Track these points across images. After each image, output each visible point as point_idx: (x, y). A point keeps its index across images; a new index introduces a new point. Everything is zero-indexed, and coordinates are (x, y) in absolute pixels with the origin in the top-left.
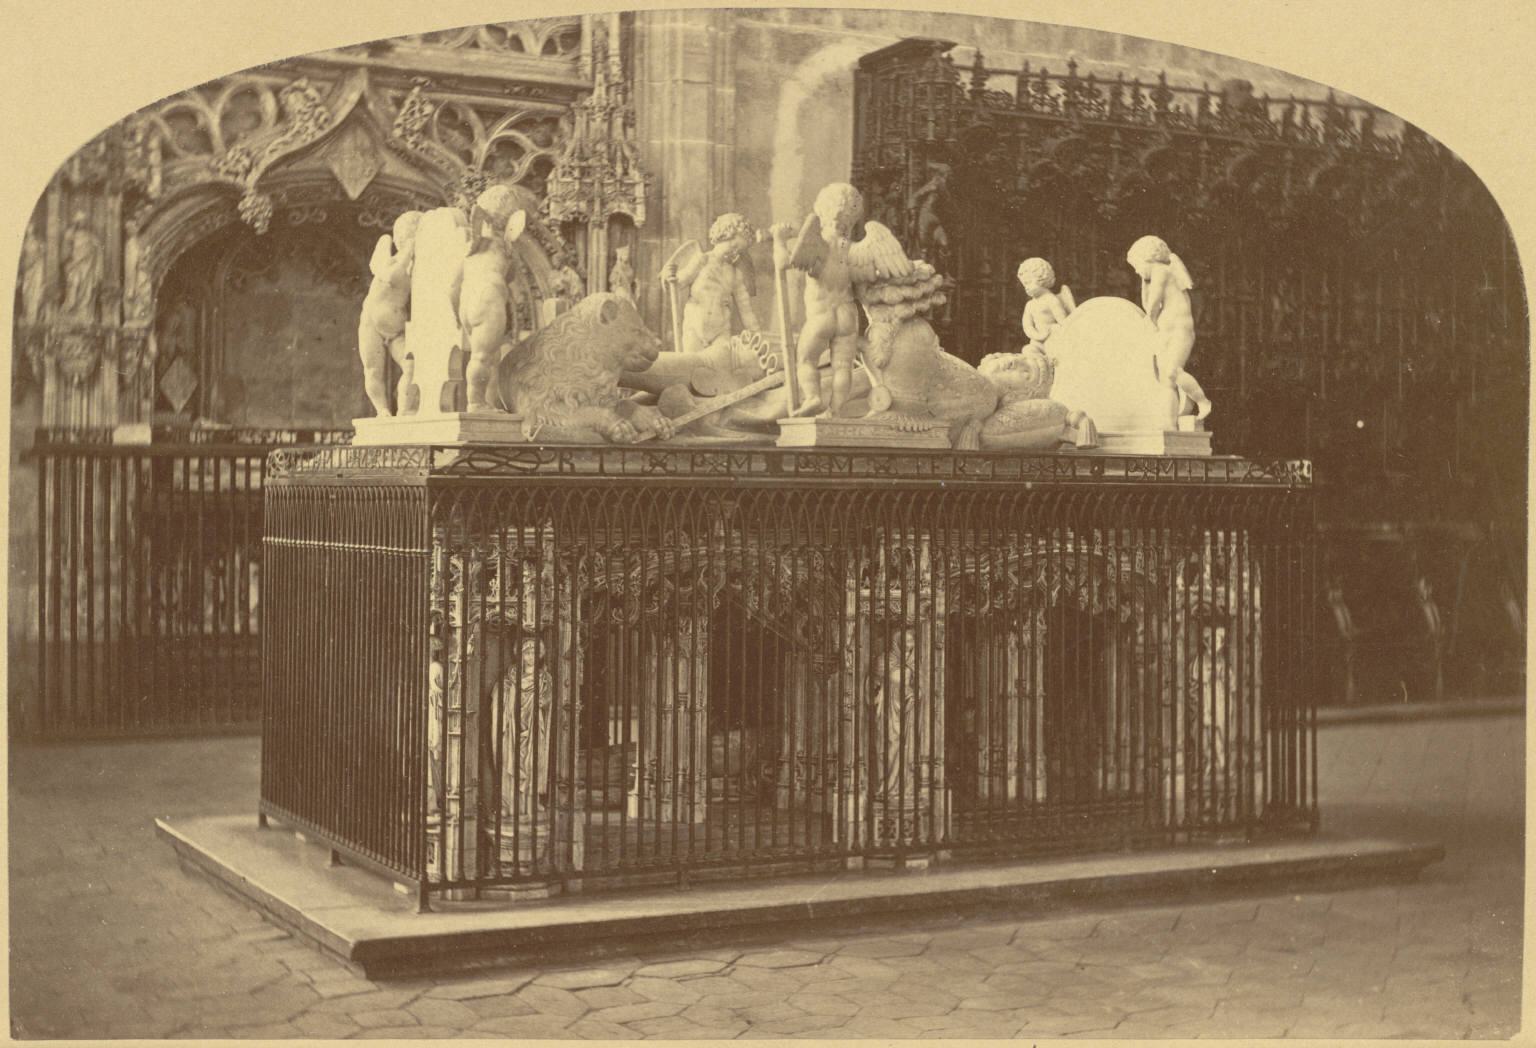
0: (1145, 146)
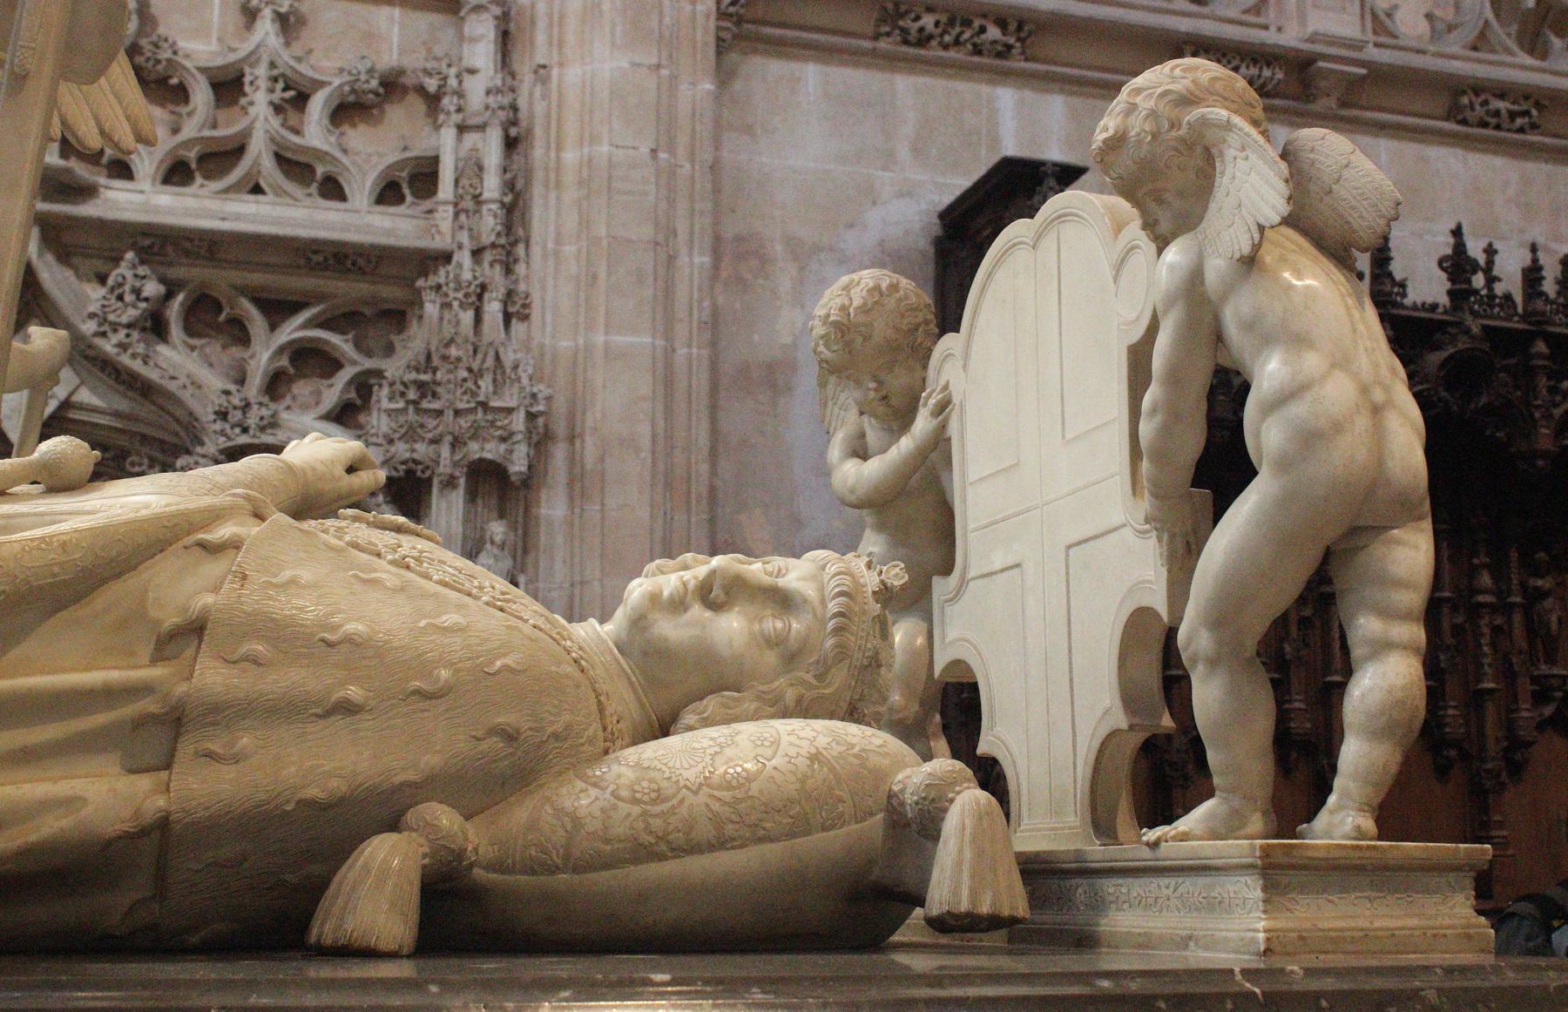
0: (1437, 347)
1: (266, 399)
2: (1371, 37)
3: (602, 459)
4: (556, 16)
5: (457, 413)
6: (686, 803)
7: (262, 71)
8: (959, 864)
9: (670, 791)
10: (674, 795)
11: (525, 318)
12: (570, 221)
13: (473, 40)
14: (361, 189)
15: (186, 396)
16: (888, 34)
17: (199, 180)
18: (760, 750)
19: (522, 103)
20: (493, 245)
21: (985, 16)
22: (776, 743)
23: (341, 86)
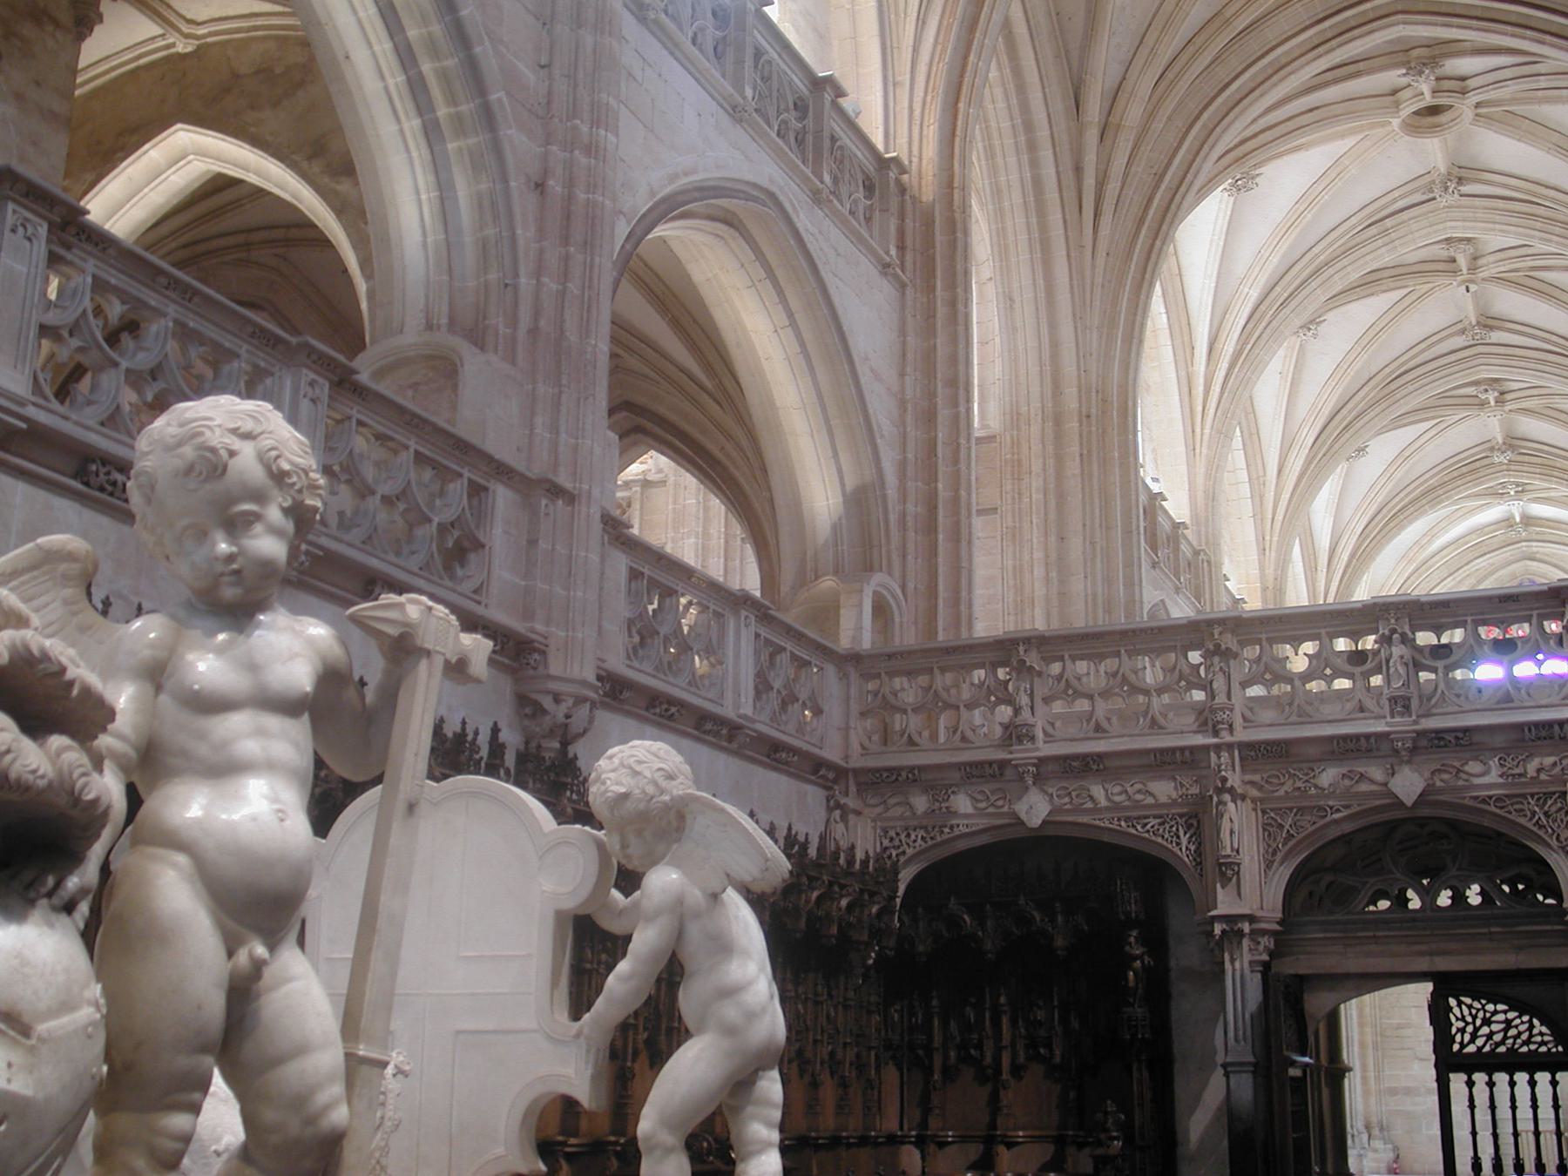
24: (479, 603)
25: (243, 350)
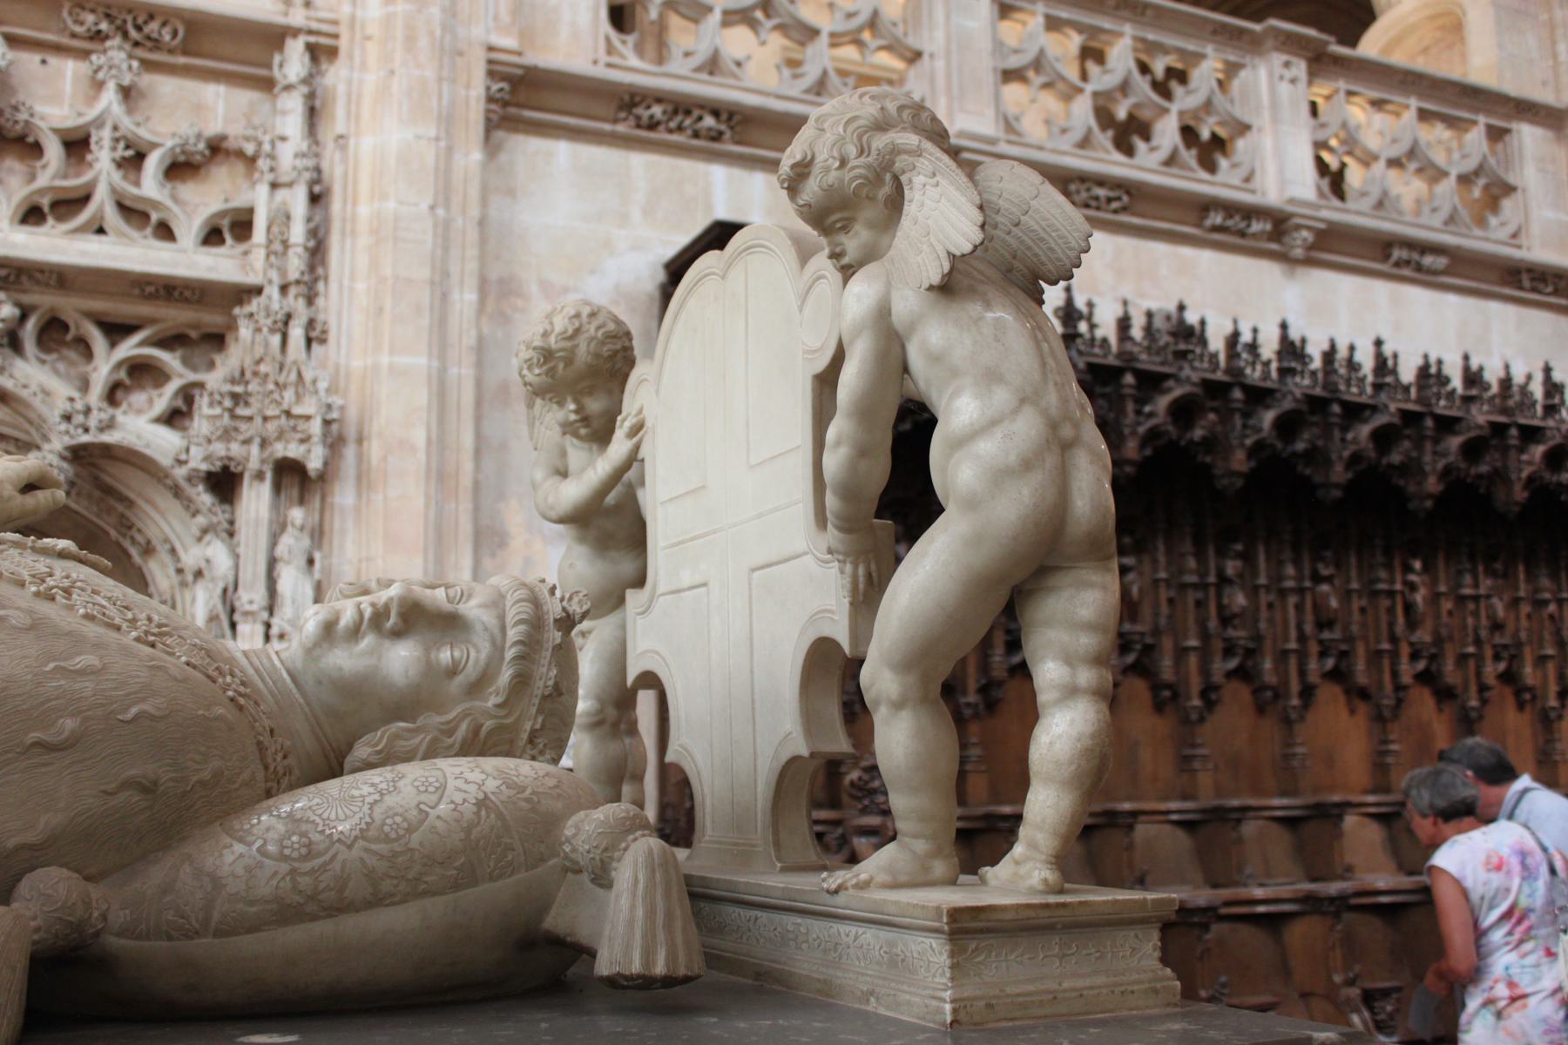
1: (105, 405)
2: (1001, 134)
3: (384, 459)
4: (354, 97)
5: (265, 419)
6: (340, 858)
7: (106, 134)
8: (631, 922)
9: (322, 847)
10: (327, 850)
11: (323, 341)
12: (363, 261)
13: (284, 113)
14: (189, 229)
15: (37, 402)
16: (625, 120)
17: (51, 221)
18: (423, 797)
19: (325, 165)
20: (298, 282)
21: (702, 107)
22: (442, 789)
23: (172, 149)
24: (1519, 247)
25: (1209, 49)
